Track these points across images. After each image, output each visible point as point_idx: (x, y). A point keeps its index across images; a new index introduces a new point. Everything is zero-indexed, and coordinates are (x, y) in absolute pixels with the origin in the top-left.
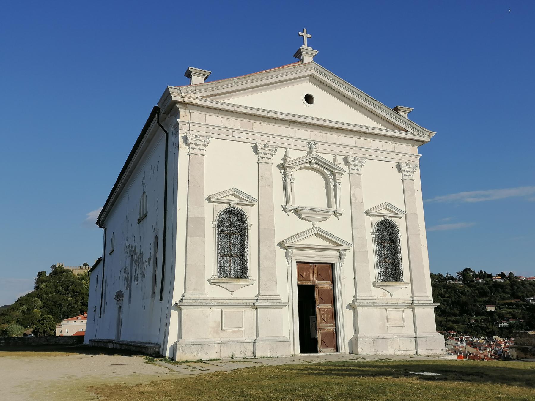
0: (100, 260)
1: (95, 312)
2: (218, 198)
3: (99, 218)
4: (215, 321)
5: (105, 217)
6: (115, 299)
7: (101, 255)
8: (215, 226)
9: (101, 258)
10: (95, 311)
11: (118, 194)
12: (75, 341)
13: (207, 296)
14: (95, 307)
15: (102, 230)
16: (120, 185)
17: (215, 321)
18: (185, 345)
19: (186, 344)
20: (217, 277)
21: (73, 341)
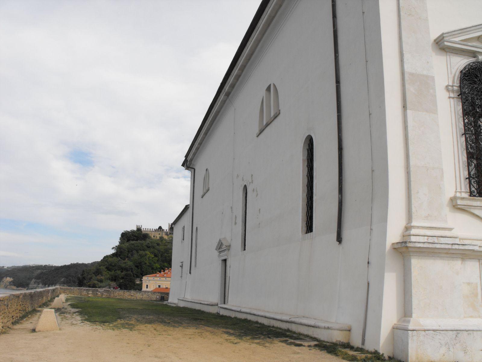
0: (187, 207)
1: (182, 268)
2: (457, 39)
3: (187, 156)
4: (469, 284)
5: (195, 154)
6: (216, 249)
7: (188, 203)
8: (456, 95)
9: (189, 205)
10: (182, 266)
11: (218, 112)
12: (158, 297)
13: (453, 231)
14: (182, 262)
15: (188, 173)
16: (222, 96)
17: (469, 284)
18: (425, 330)
19: (426, 328)
20: (466, 195)
21: (156, 297)
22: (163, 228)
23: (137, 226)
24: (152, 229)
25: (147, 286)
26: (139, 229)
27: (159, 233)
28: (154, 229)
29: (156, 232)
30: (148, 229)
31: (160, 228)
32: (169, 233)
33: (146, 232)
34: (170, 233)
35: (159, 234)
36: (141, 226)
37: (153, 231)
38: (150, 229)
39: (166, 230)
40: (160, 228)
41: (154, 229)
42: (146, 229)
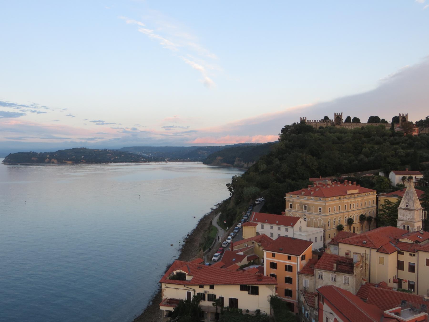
22: (330, 118)
23: (301, 118)
24: (317, 120)
25: (291, 205)
26: (303, 121)
27: (324, 124)
28: (320, 120)
29: (321, 124)
30: (313, 120)
31: (326, 118)
32: (335, 123)
33: (311, 124)
34: (336, 123)
35: (325, 124)
36: (306, 118)
37: (318, 123)
38: (315, 120)
39: (332, 120)
40: (326, 118)
41: (320, 120)
42: (310, 120)
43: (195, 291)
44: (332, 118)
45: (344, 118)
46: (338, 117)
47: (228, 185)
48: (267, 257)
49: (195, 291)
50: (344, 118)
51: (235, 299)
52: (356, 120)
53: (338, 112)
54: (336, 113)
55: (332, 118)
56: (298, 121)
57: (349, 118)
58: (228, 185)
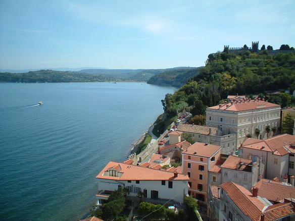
31: (245, 46)
40: (245, 46)
43: (124, 185)
44: (250, 46)
45: (260, 48)
46: (255, 46)
47: (162, 101)
48: (184, 158)
49: (124, 185)
50: (260, 48)
51: (155, 191)
52: (270, 48)
53: (255, 41)
54: (254, 42)
55: (250, 46)
56: (222, 50)
57: (264, 46)
58: (162, 101)
